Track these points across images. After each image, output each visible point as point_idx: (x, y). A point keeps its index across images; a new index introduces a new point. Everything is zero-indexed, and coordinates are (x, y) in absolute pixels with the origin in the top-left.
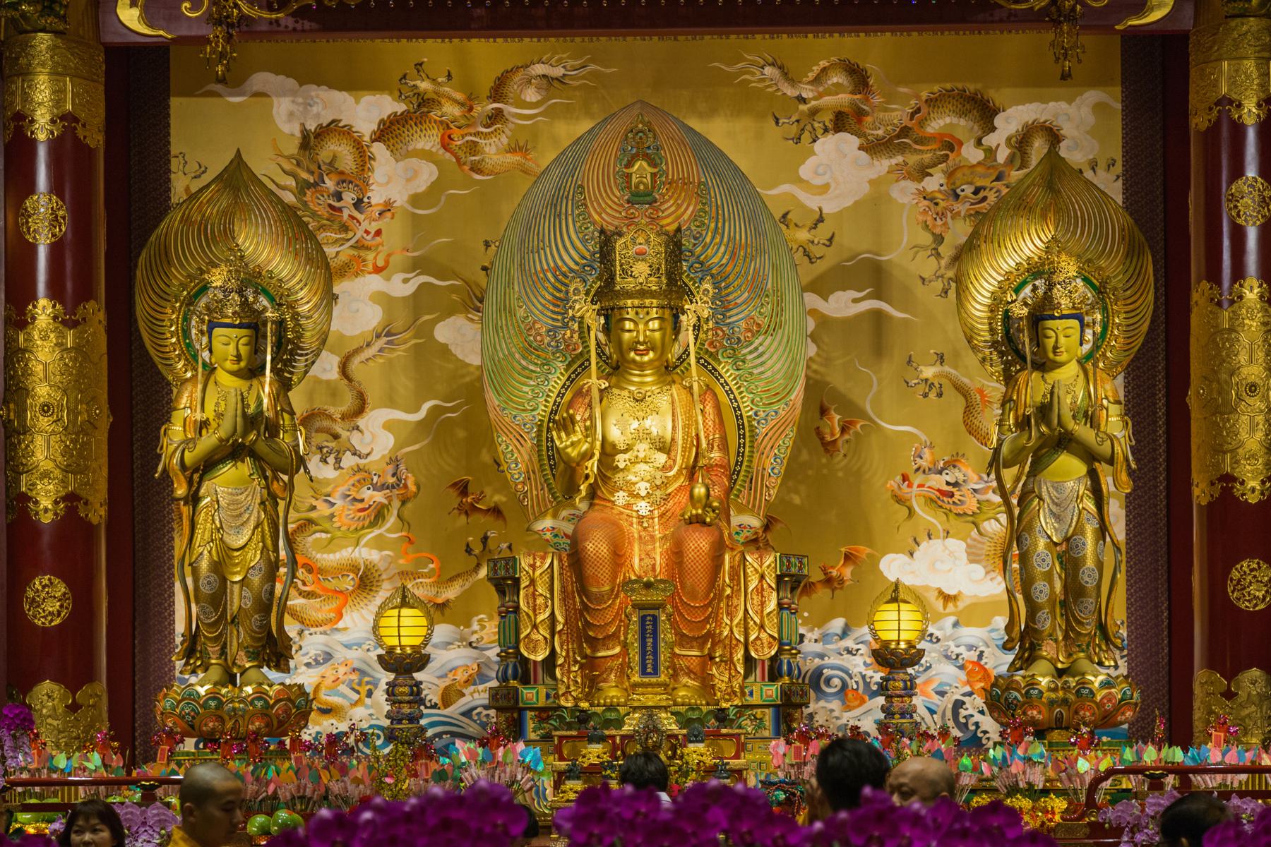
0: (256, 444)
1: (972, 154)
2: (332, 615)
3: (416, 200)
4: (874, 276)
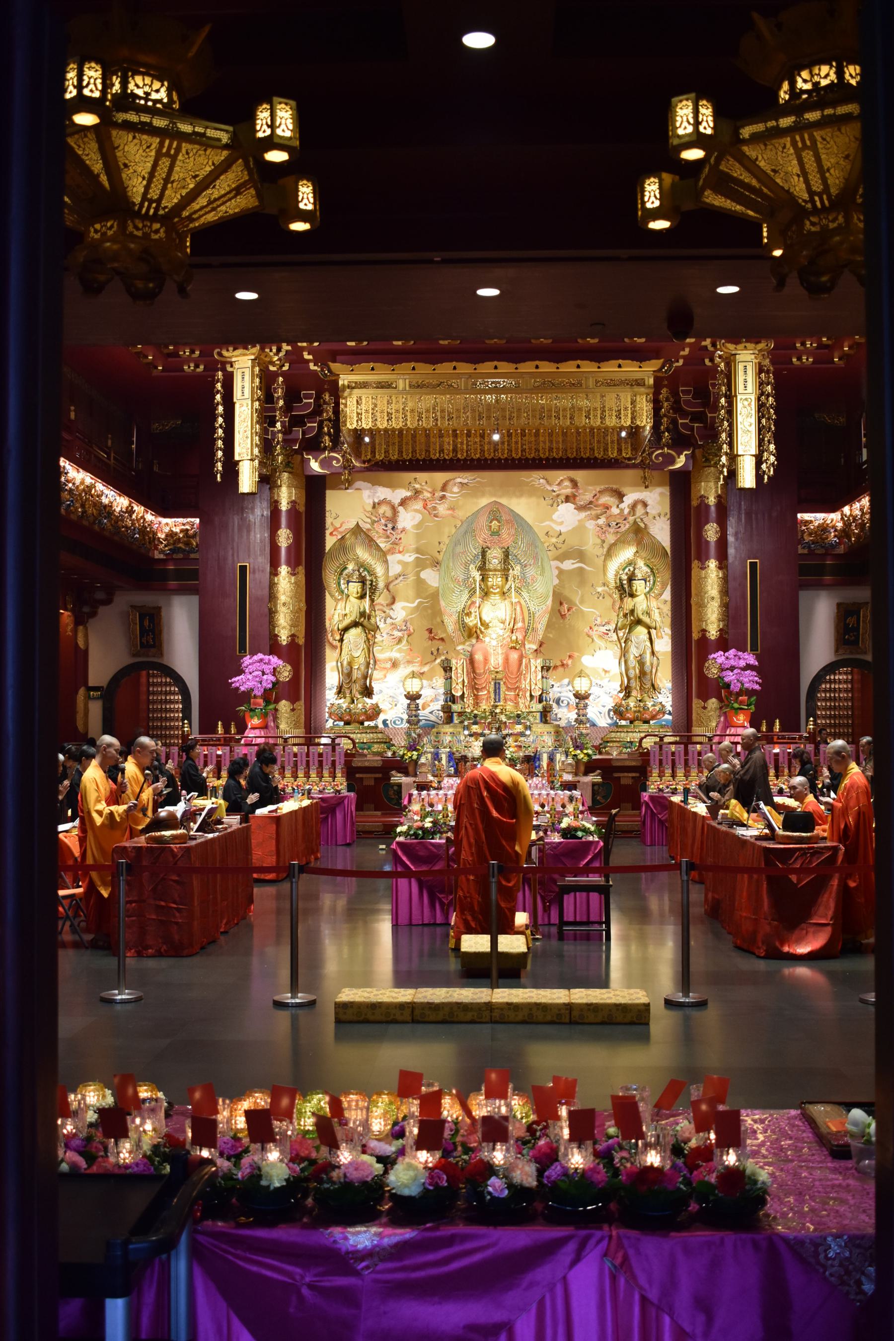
0: (363, 622)
1: (615, 511)
4: (580, 555)
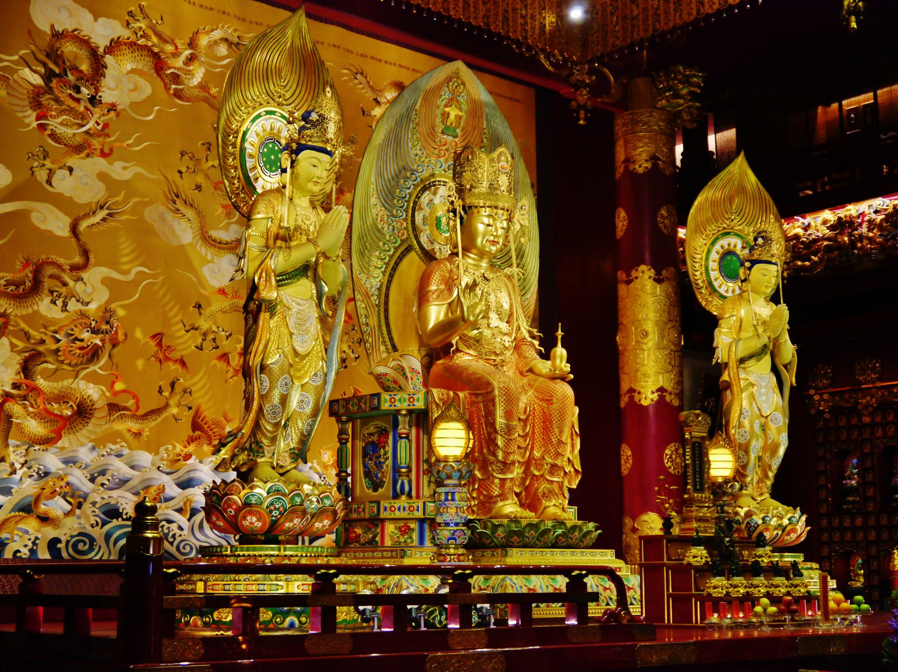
2: (53, 435)
3: (134, 105)
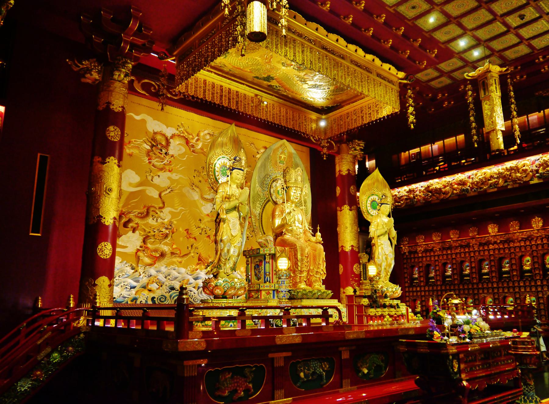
3: (179, 155)
